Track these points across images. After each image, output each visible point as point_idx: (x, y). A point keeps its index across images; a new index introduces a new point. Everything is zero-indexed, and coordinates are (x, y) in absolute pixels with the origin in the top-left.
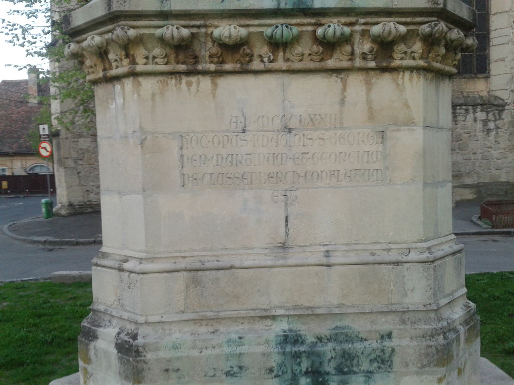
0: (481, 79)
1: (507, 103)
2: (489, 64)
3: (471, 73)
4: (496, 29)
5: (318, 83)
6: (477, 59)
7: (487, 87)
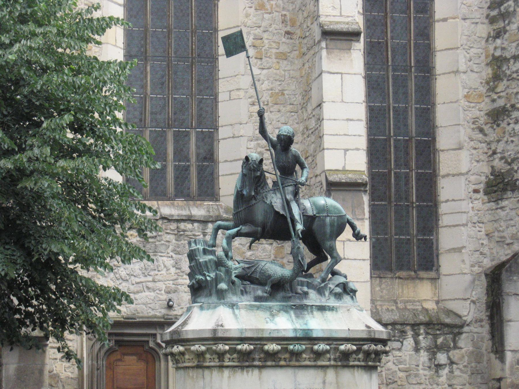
0: (425, 282)
1: (465, 321)
2: (437, 256)
3: (409, 269)
4: (447, 201)
5: (312, 372)
6: (418, 247)
7: (435, 294)
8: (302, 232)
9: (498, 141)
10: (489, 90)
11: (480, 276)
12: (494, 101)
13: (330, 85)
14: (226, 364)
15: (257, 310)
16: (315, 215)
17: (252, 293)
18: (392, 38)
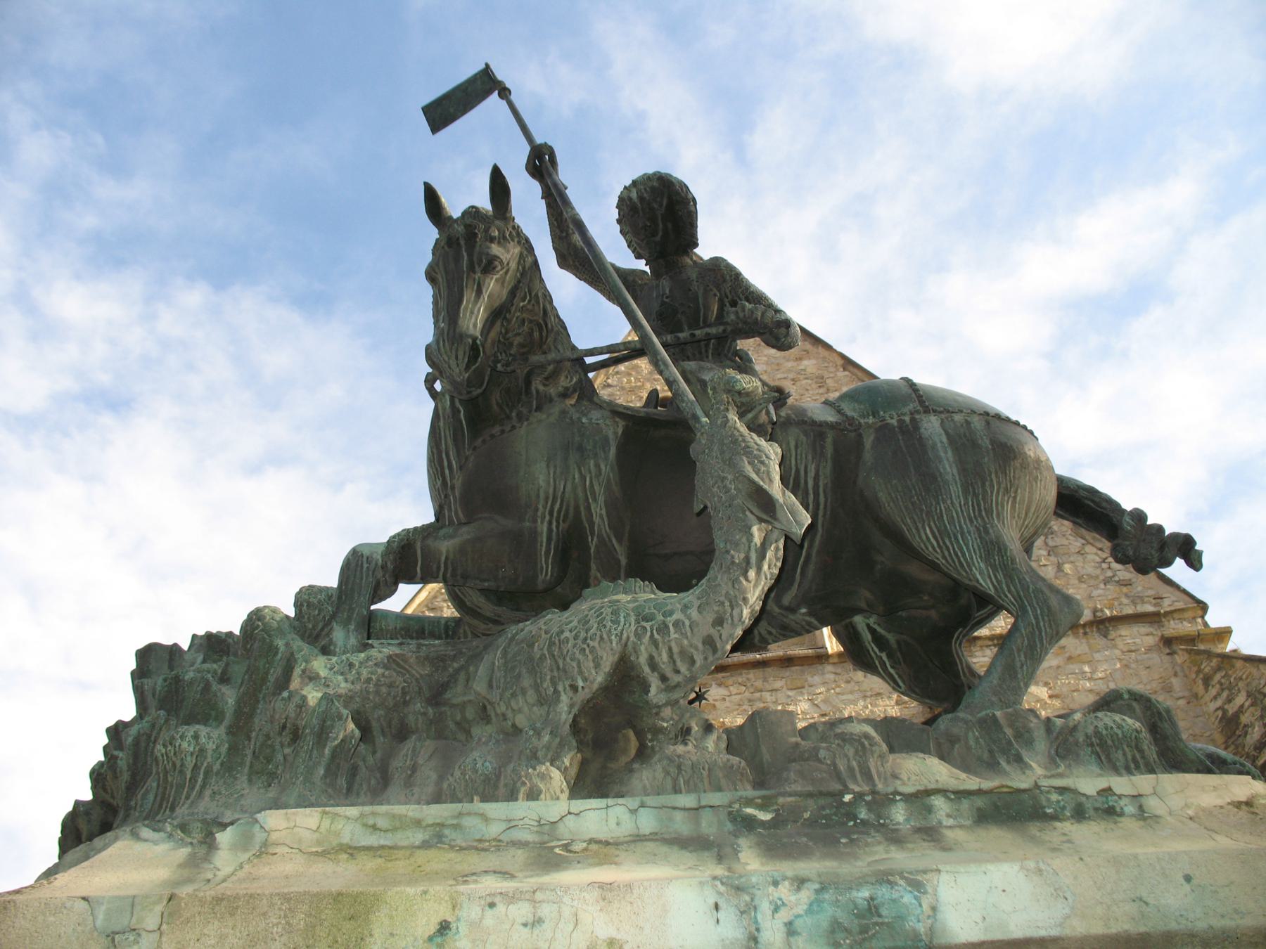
15: (425, 845)
16: (851, 420)
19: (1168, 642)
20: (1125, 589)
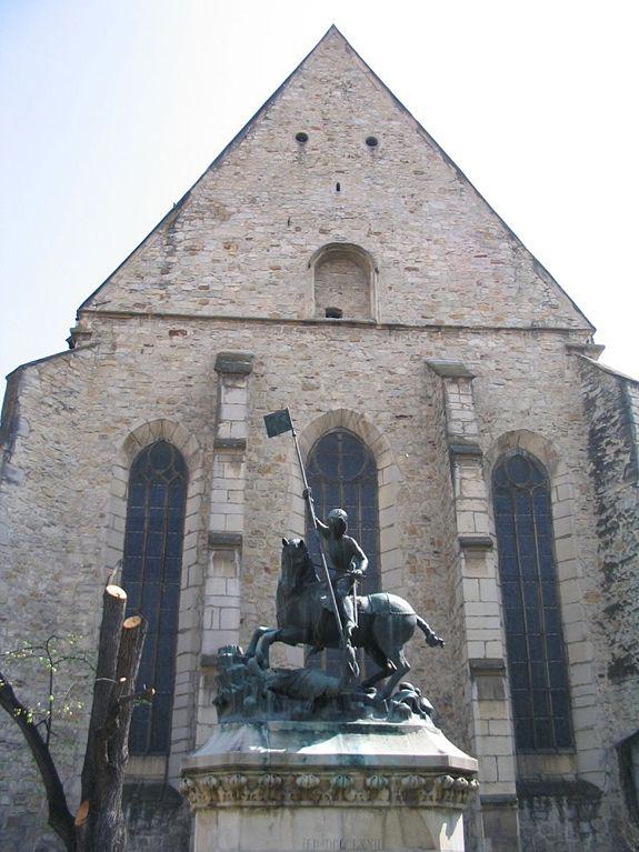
4: (577, 686)
5: (365, 816)
8: (354, 630)
9: (615, 633)
10: (604, 591)
11: (612, 751)
12: (609, 599)
13: (469, 589)
14: (245, 803)
17: (290, 709)
18: (521, 554)
19: (569, 348)
20: (553, 311)
